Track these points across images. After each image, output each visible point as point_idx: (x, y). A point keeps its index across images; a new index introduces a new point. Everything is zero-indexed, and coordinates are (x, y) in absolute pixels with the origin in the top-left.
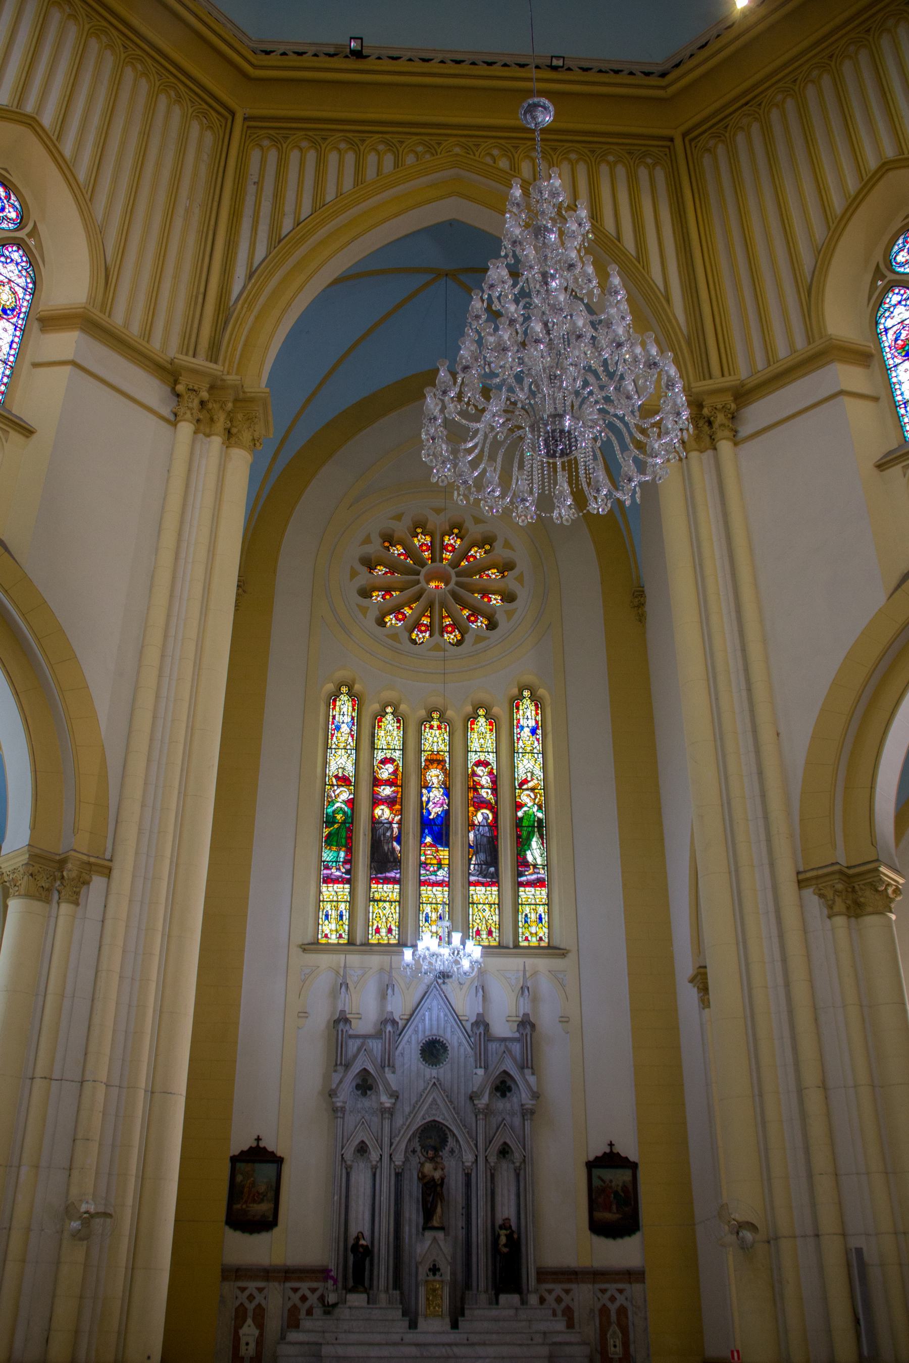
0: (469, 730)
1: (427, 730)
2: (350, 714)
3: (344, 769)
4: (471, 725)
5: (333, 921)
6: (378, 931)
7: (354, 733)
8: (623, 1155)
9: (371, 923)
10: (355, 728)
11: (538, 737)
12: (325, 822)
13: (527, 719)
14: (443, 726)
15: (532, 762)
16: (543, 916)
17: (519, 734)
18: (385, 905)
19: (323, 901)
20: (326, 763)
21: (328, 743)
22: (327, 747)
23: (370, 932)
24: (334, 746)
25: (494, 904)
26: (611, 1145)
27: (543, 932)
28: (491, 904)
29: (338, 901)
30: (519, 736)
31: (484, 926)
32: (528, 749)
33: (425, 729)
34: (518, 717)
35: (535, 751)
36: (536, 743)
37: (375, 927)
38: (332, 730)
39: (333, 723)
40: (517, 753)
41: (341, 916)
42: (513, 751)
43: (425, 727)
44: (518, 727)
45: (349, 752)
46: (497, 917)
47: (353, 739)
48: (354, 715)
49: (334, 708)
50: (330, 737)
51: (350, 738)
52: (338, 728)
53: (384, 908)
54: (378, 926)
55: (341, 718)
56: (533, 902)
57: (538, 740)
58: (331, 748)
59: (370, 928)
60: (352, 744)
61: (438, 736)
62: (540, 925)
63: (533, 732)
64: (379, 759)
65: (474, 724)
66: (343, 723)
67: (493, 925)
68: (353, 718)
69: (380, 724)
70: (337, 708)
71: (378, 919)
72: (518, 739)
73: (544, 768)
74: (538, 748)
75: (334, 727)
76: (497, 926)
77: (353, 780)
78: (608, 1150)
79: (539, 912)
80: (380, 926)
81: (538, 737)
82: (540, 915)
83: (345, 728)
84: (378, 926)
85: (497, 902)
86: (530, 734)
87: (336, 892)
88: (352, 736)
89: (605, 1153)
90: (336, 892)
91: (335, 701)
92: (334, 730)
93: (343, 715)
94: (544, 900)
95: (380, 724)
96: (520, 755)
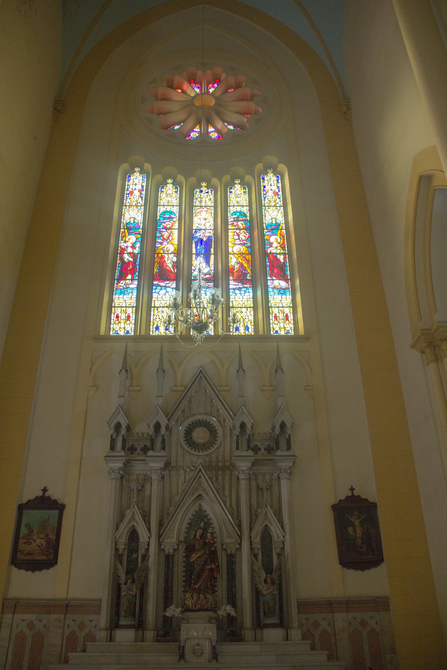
0: (229, 193)
1: (198, 193)
2: (140, 184)
3: (135, 219)
4: (230, 190)
5: (122, 321)
6: (157, 328)
7: (143, 196)
8: (363, 497)
9: (152, 323)
10: (144, 193)
11: (279, 196)
12: (119, 254)
13: (271, 185)
14: (210, 191)
15: (276, 212)
16: (289, 315)
17: (265, 194)
18: (163, 309)
19: (115, 307)
20: (121, 214)
21: (123, 202)
22: (122, 204)
23: (151, 330)
24: (128, 204)
25: (250, 307)
26: (352, 489)
27: (290, 326)
28: (247, 308)
29: (126, 307)
30: (265, 196)
31: (242, 324)
32: (273, 204)
33: (196, 193)
34: (264, 185)
35: (278, 205)
36: (278, 201)
37: (155, 326)
38: (127, 194)
39: (128, 190)
40: (264, 206)
41: (129, 317)
42: (260, 206)
43: (196, 192)
44: (264, 190)
45: (139, 207)
46: (252, 317)
47: (142, 200)
48: (143, 184)
49: (129, 181)
50: (125, 198)
51: (140, 199)
52: (132, 193)
53: (163, 312)
54: (157, 325)
55: (134, 187)
56: (281, 305)
57: (279, 198)
58: (126, 206)
59: (151, 327)
60: (141, 202)
61: (206, 197)
62: (287, 322)
63: (276, 194)
64: (161, 211)
65: (232, 189)
66: (135, 189)
67: (249, 323)
68: (142, 187)
69: (162, 190)
70: (131, 181)
71: (158, 320)
72: (265, 198)
73: (286, 215)
74: (279, 203)
75: (128, 192)
76: (253, 323)
77: (141, 226)
78: (350, 494)
79: (286, 312)
80: (159, 325)
81: (279, 196)
82: (287, 315)
83: (136, 193)
84: (157, 325)
85: (252, 305)
86: (273, 195)
87: (125, 301)
88: (142, 198)
89: (347, 497)
90: (125, 301)
91: (130, 176)
92: (128, 194)
93: (136, 185)
94: (289, 304)
95: (162, 190)
96: (267, 208)
